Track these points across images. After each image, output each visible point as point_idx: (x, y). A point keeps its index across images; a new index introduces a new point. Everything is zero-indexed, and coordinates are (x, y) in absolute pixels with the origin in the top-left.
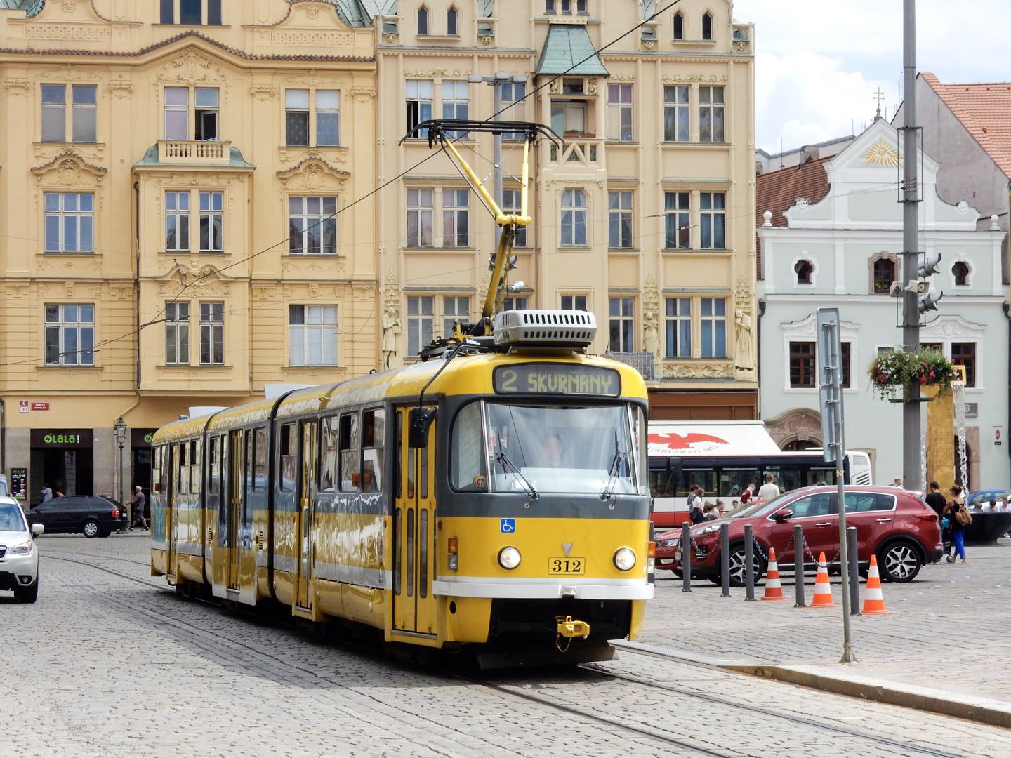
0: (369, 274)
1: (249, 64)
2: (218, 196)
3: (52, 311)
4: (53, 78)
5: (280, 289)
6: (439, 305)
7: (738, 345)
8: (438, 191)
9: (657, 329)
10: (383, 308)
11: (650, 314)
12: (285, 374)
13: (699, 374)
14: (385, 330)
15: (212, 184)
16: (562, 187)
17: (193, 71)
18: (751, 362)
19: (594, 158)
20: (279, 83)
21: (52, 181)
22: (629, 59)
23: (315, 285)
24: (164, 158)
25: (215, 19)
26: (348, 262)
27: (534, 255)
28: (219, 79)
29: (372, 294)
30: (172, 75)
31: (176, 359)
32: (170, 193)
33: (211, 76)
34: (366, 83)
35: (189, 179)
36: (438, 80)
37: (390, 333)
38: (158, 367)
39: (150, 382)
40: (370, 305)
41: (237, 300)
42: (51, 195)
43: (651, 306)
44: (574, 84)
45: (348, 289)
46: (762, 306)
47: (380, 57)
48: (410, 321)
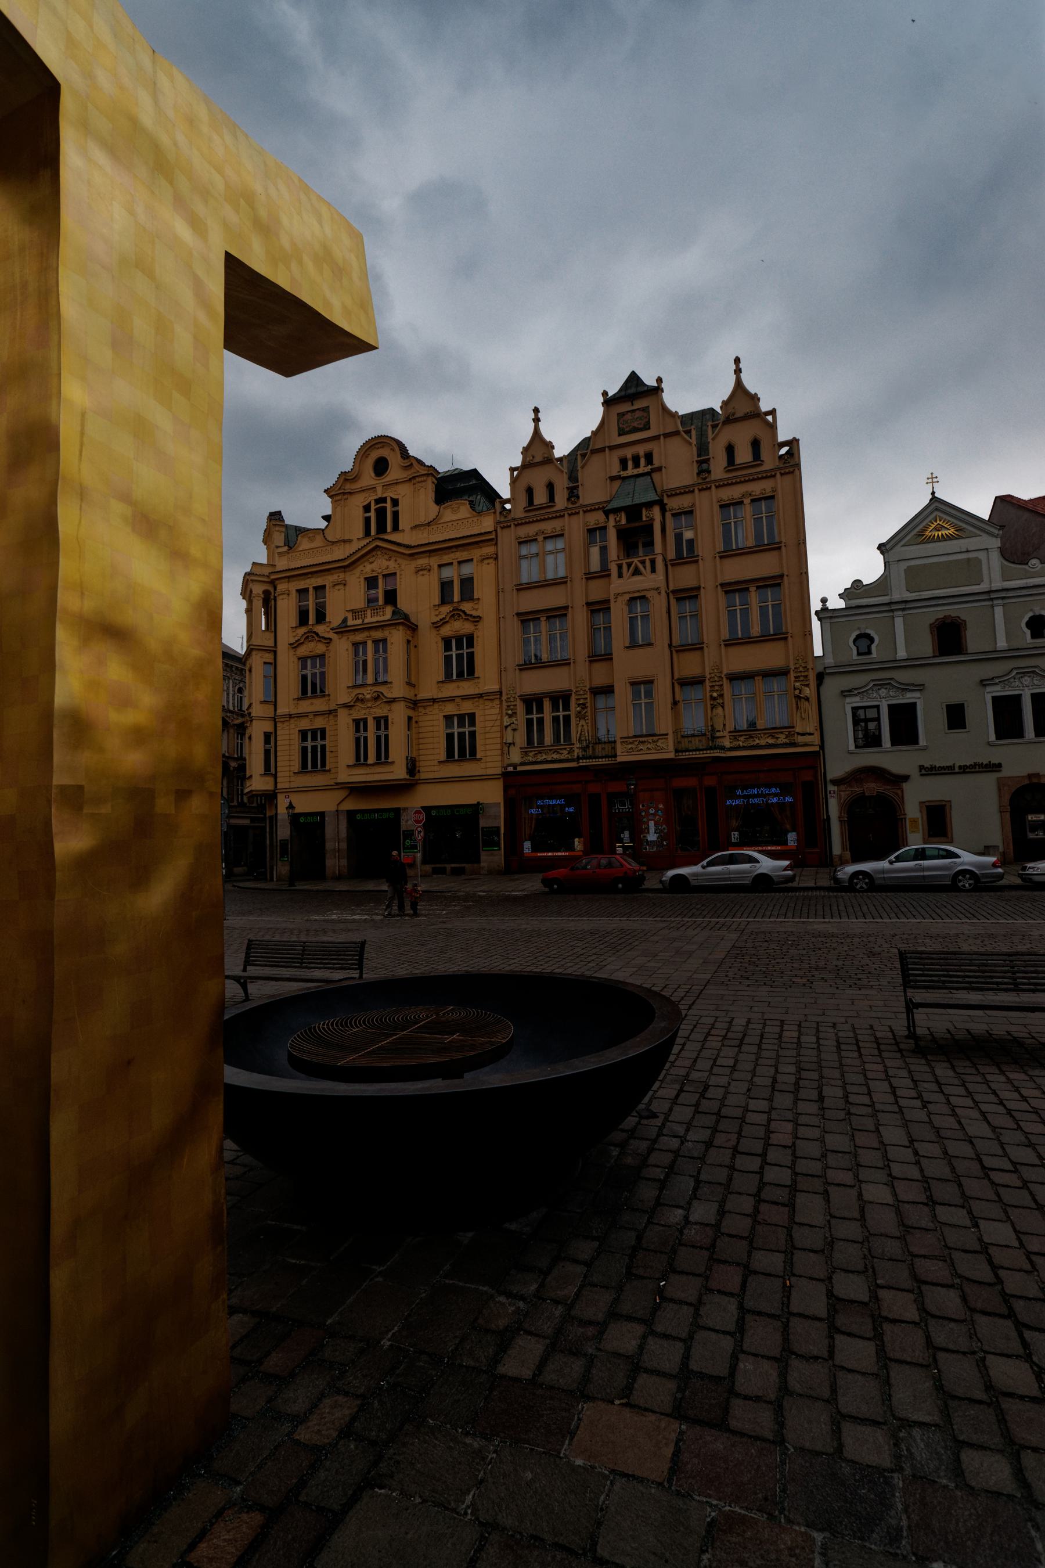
0: (494, 687)
1: (414, 552)
2: (384, 641)
3: (303, 734)
4: (302, 584)
5: (436, 706)
6: (547, 705)
9: (723, 707)
10: (504, 712)
11: (715, 694)
13: (763, 742)
14: (506, 727)
15: (378, 634)
16: (627, 597)
17: (378, 565)
18: (811, 726)
19: (653, 570)
20: (434, 561)
21: (303, 651)
22: (687, 490)
23: (458, 700)
24: (350, 622)
25: (396, 528)
29: (498, 702)
31: (360, 759)
32: (355, 645)
33: (392, 565)
34: (489, 550)
35: (366, 634)
36: (540, 538)
37: (509, 729)
38: (349, 766)
40: (497, 711)
41: (398, 715)
42: (303, 660)
43: (717, 688)
44: (633, 512)
46: (820, 677)
47: (499, 530)
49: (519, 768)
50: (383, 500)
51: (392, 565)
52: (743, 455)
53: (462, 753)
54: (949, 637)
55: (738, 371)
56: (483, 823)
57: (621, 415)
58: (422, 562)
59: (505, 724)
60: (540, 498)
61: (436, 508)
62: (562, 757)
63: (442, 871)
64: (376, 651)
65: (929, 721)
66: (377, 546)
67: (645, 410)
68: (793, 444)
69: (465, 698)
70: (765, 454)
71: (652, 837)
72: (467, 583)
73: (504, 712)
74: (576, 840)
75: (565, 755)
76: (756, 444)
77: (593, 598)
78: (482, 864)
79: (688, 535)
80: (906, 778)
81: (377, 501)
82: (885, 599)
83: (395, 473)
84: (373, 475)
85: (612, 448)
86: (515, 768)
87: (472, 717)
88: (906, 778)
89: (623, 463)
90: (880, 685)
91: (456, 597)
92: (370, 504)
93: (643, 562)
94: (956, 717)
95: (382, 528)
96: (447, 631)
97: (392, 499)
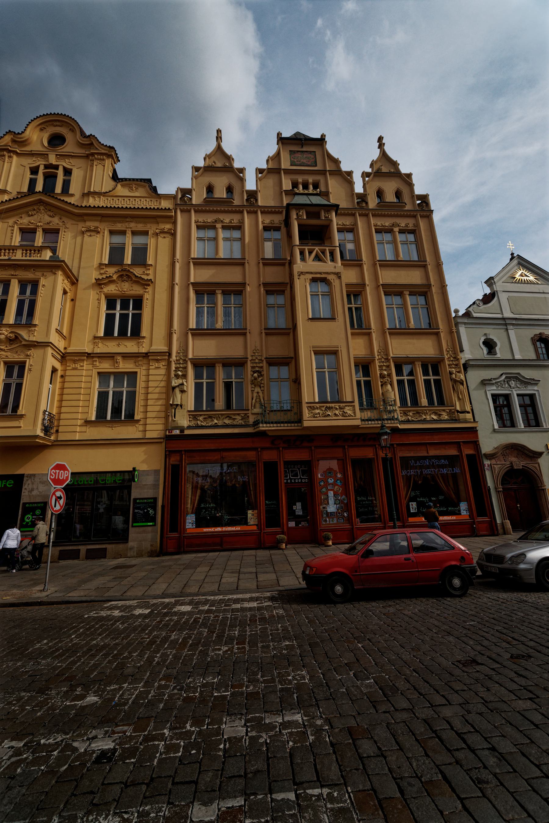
0: (165, 349)
2: (35, 284)
7: (456, 395)
8: (219, 292)
10: (173, 373)
12: (88, 427)
15: (29, 275)
16: (311, 276)
17: (41, 219)
19: (333, 259)
20: (105, 228)
26: (146, 342)
27: (291, 334)
28: (61, 224)
30: (25, 221)
33: (56, 222)
37: (177, 390)
40: (163, 371)
43: (384, 368)
44: (314, 211)
45: (145, 361)
48: (196, 384)
49: (187, 432)
50: (56, 167)
51: (56, 222)
53: (117, 411)
56: (136, 493)
58: (92, 224)
59: (174, 384)
62: (235, 423)
63: (75, 555)
64: (22, 291)
66: (40, 202)
68: (424, 199)
69: (126, 356)
70: (406, 198)
71: (332, 508)
72: (140, 255)
73: (173, 373)
74: (250, 512)
75: (239, 420)
77: (270, 279)
78: (131, 544)
80: (540, 454)
82: (500, 316)
83: (69, 147)
84: (46, 144)
86: (182, 430)
87: (133, 376)
88: (540, 454)
89: (295, 185)
90: (509, 378)
91: (128, 260)
92: (38, 167)
93: (323, 252)
96: (111, 289)
97: (64, 168)
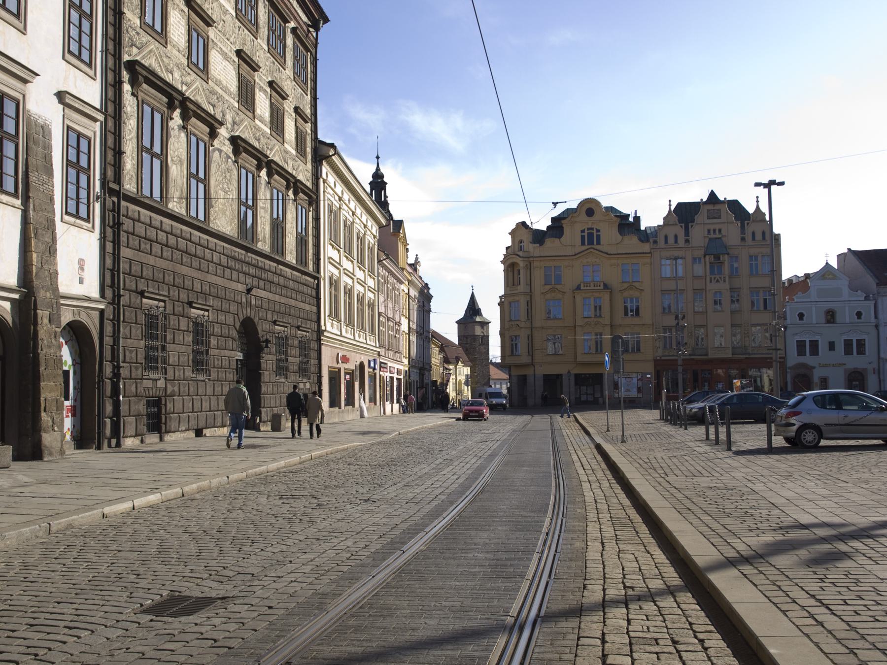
15: (597, 295)
21: (548, 296)
25: (598, 243)
39: (579, 359)
50: (592, 229)
52: (759, 237)
54: (831, 316)
55: (758, 202)
57: (708, 210)
60: (671, 240)
61: (619, 237)
65: (823, 347)
67: (719, 210)
76: (764, 233)
79: (736, 265)
80: (814, 368)
81: (588, 229)
83: (596, 216)
85: (705, 224)
88: (814, 368)
89: (709, 231)
94: (832, 346)
95: (591, 242)
